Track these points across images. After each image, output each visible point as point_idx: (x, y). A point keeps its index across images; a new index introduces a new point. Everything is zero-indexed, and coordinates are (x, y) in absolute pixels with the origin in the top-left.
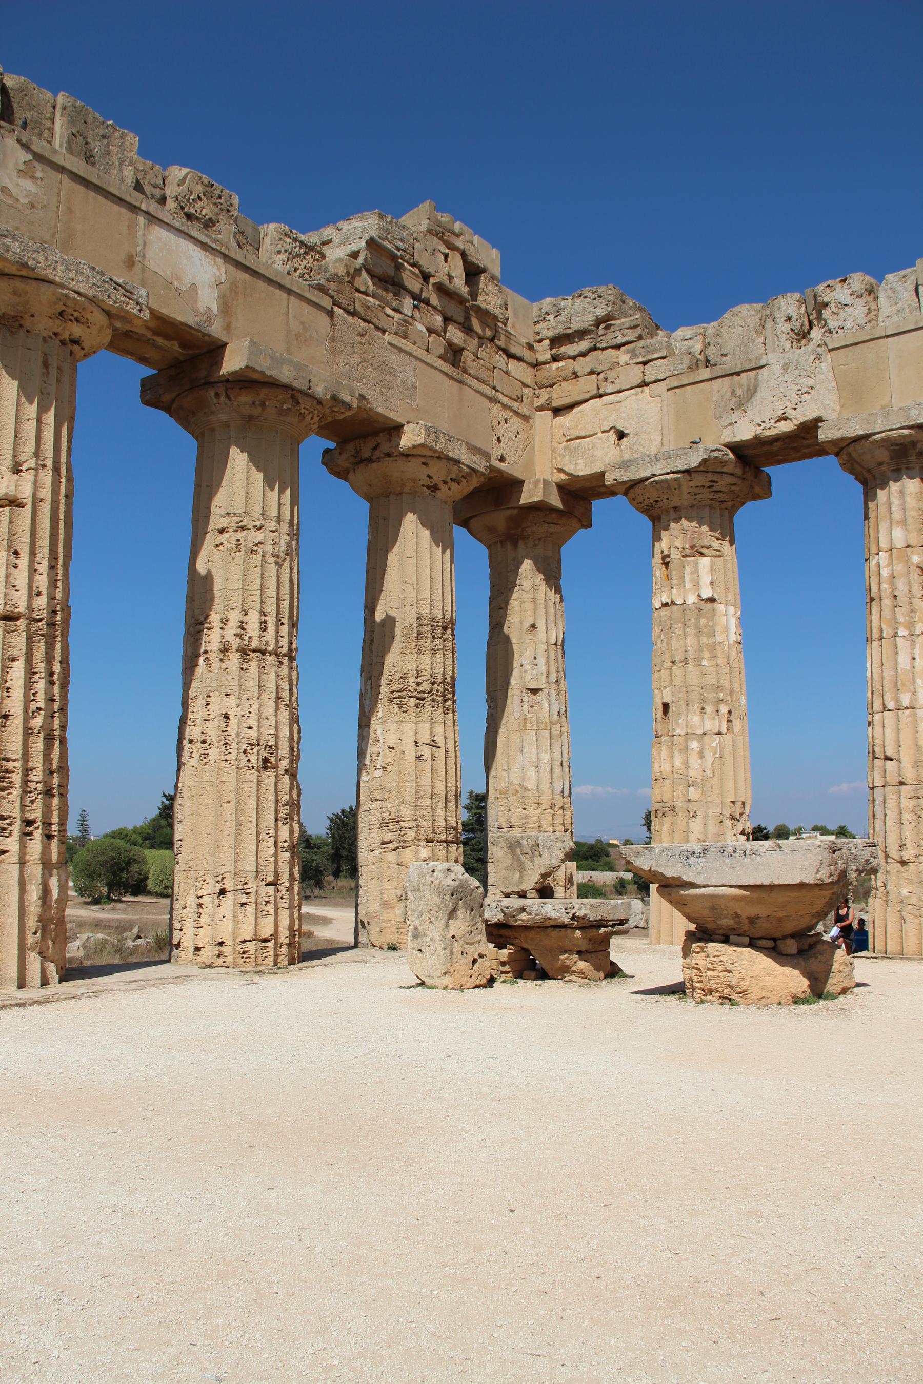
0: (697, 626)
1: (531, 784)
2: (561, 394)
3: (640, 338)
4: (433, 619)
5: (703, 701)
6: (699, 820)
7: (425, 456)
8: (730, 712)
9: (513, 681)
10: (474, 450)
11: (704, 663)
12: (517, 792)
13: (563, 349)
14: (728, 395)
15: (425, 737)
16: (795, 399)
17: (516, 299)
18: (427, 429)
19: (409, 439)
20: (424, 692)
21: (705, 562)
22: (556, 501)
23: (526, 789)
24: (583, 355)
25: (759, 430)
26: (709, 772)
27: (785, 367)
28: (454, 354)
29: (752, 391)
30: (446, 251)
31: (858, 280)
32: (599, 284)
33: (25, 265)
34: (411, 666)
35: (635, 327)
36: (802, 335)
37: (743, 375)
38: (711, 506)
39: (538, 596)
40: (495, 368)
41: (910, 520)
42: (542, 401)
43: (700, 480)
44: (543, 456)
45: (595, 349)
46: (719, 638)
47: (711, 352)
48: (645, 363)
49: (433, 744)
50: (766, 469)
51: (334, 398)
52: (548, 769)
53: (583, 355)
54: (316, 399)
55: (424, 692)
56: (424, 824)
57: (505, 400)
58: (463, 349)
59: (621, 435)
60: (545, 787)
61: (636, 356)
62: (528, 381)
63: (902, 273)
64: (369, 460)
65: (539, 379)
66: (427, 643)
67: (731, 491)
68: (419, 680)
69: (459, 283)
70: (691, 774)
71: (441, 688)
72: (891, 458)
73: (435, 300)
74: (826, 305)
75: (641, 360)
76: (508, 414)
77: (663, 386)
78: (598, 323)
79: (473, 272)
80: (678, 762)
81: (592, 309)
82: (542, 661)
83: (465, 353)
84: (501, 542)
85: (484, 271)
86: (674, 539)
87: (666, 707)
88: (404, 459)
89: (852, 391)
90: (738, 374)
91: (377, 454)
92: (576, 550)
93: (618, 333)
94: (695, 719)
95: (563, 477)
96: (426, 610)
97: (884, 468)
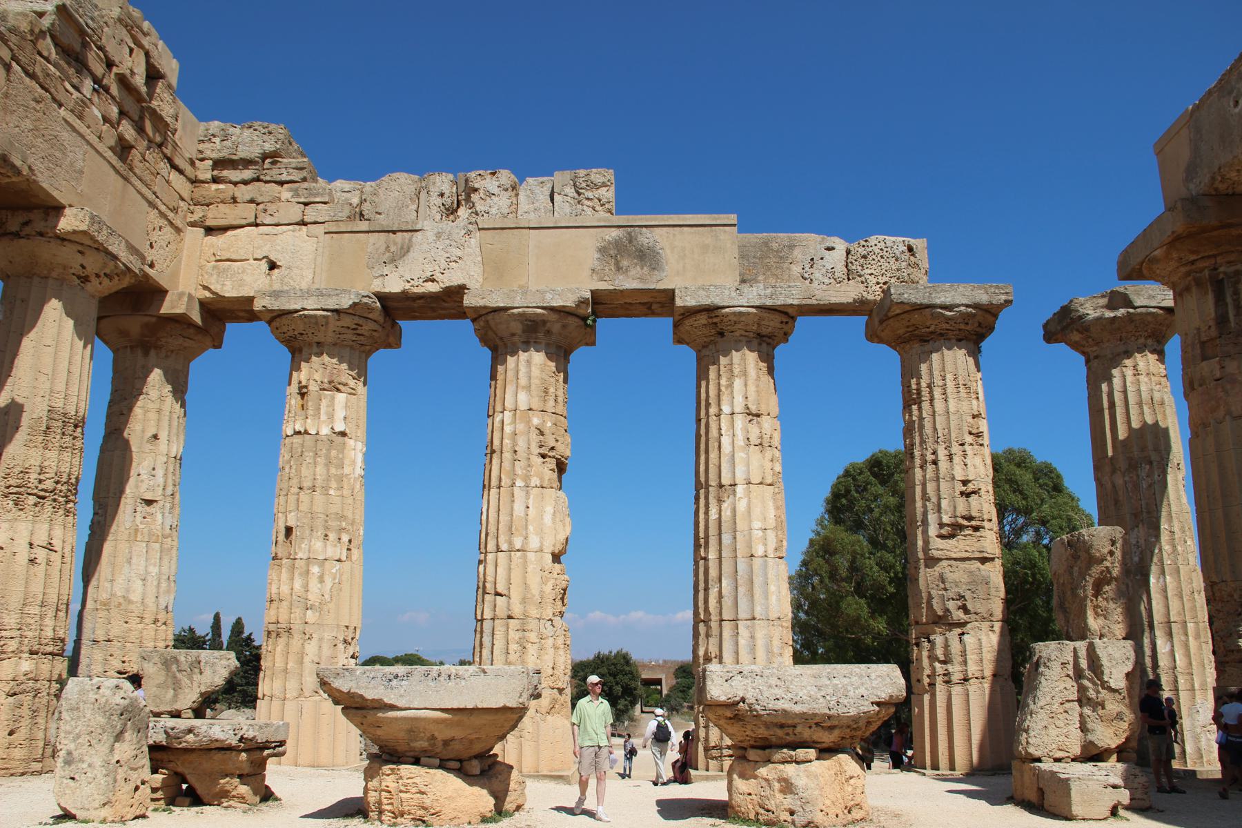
0: (328, 457)
1: (135, 597)
2: (217, 216)
3: (304, 180)
4: (65, 415)
5: (327, 528)
6: (314, 642)
8: (350, 541)
9: (129, 490)
10: (133, 250)
11: (331, 492)
12: (120, 604)
13: (225, 173)
14: (383, 249)
15: (41, 538)
16: (444, 265)
17: (186, 114)
18: (93, 217)
19: (68, 222)
20: (46, 491)
21: (341, 398)
22: (196, 317)
23: (130, 602)
24: (245, 183)
25: (407, 286)
26: (327, 596)
27: (438, 236)
28: (123, 149)
29: (406, 250)
30: (133, 46)
31: (505, 176)
32: (271, 122)
34: (34, 461)
35: (302, 169)
36: (451, 211)
37: (399, 234)
38: (352, 347)
39: (163, 407)
41: (533, 387)
42: (196, 217)
43: (347, 321)
44: (190, 271)
45: (258, 180)
46: (347, 470)
47: (366, 208)
48: (306, 204)
49: (50, 547)
50: (401, 323)
52: (155, 583)
53: (245, 183)
55: (46, 491)
56: (30, 634)
57: (163, 208)
58: (132, 147)
59: (273, 266)
60: (150, 601)
61: (298, 196)
62: (186, 195)
63: (541, 179)
64: (17, 235)
65: (196, 196)
66: (56, 439)
67: (372, 337)
68: (42, 477)
69: (139, 81)
70: (310, 597)
71: (64, 488)
72: (524, 331)
73: (114, 90)
74: (476, 190)
75: (302, 200)
76: (163, 222)
77: (320, 229)
78: (265, 156)
79: (154, 75)
80: (298, 585)
81: (260, 142)
82: (160, 472)
83: (134, 151)
84: (132, 347)
86: (313, 371)
87: (289, 531)
88: (59, 242)
89: (495, 267)
90: (394, 232)
91: (27, 230)
92: (204, 366)
93: (283, 171)
94: (318, 545)
95: (208, 294)
96: (59, 404)
97: (516, 339)
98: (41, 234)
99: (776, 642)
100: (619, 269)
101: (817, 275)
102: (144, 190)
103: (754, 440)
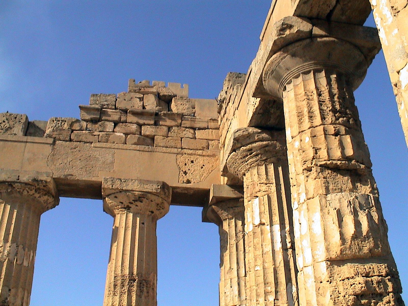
7: (114, 193)
10: (141, 181)
40: (182, 138)
51: (35, 180)
54: (23, 183)
57: (190, 152)
58: (154, 136)
66: (118, 289)
79: (165, 101)
85: (175, 96)
102: (169, 150)
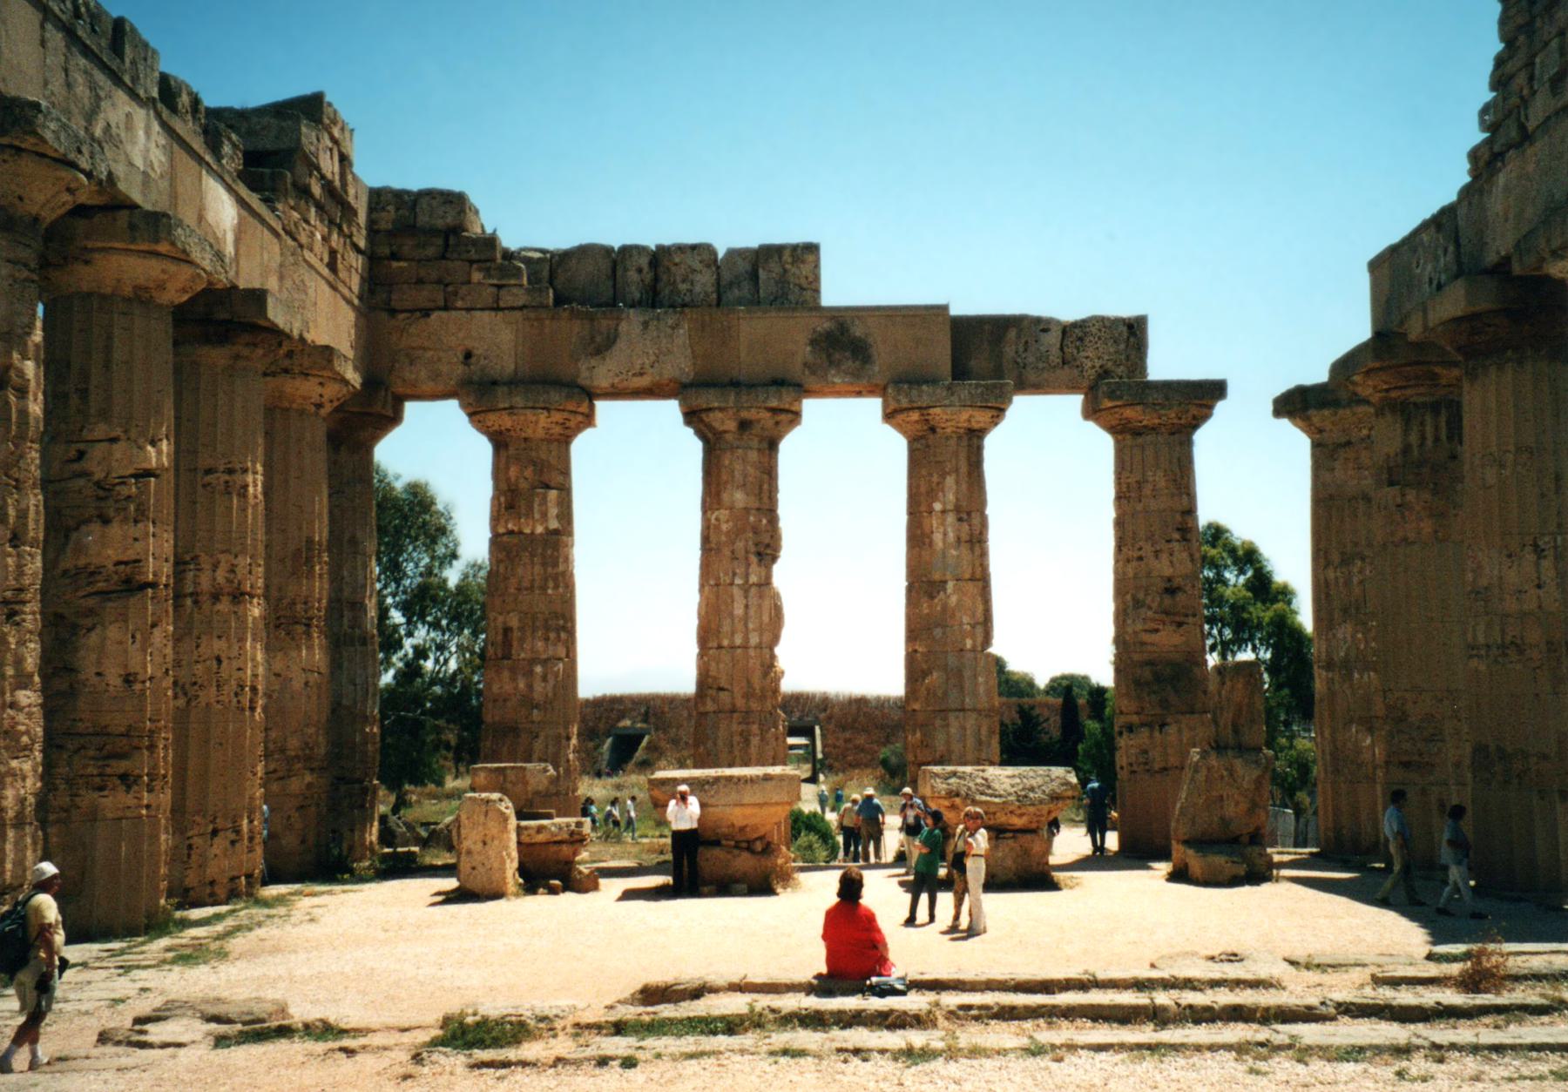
0: (543, 556)
27: (646, 325)
33: (184, 251)
48: (499, 287)
61: (490, 276)
80: (522, 685)
94: (540, 645)
98: (286, 371)
99: (984, 731)
100: (831, 363)
101: (1031, 359)
103: (965, 537)
